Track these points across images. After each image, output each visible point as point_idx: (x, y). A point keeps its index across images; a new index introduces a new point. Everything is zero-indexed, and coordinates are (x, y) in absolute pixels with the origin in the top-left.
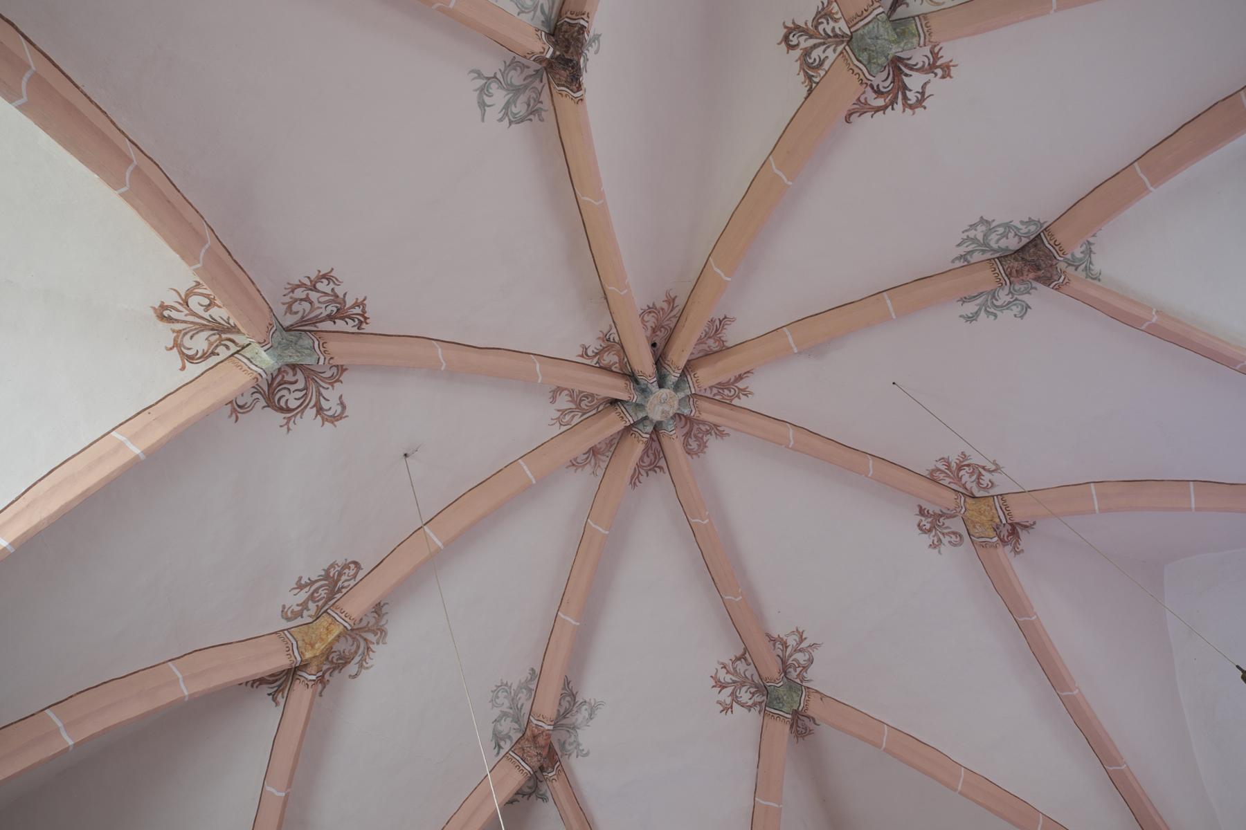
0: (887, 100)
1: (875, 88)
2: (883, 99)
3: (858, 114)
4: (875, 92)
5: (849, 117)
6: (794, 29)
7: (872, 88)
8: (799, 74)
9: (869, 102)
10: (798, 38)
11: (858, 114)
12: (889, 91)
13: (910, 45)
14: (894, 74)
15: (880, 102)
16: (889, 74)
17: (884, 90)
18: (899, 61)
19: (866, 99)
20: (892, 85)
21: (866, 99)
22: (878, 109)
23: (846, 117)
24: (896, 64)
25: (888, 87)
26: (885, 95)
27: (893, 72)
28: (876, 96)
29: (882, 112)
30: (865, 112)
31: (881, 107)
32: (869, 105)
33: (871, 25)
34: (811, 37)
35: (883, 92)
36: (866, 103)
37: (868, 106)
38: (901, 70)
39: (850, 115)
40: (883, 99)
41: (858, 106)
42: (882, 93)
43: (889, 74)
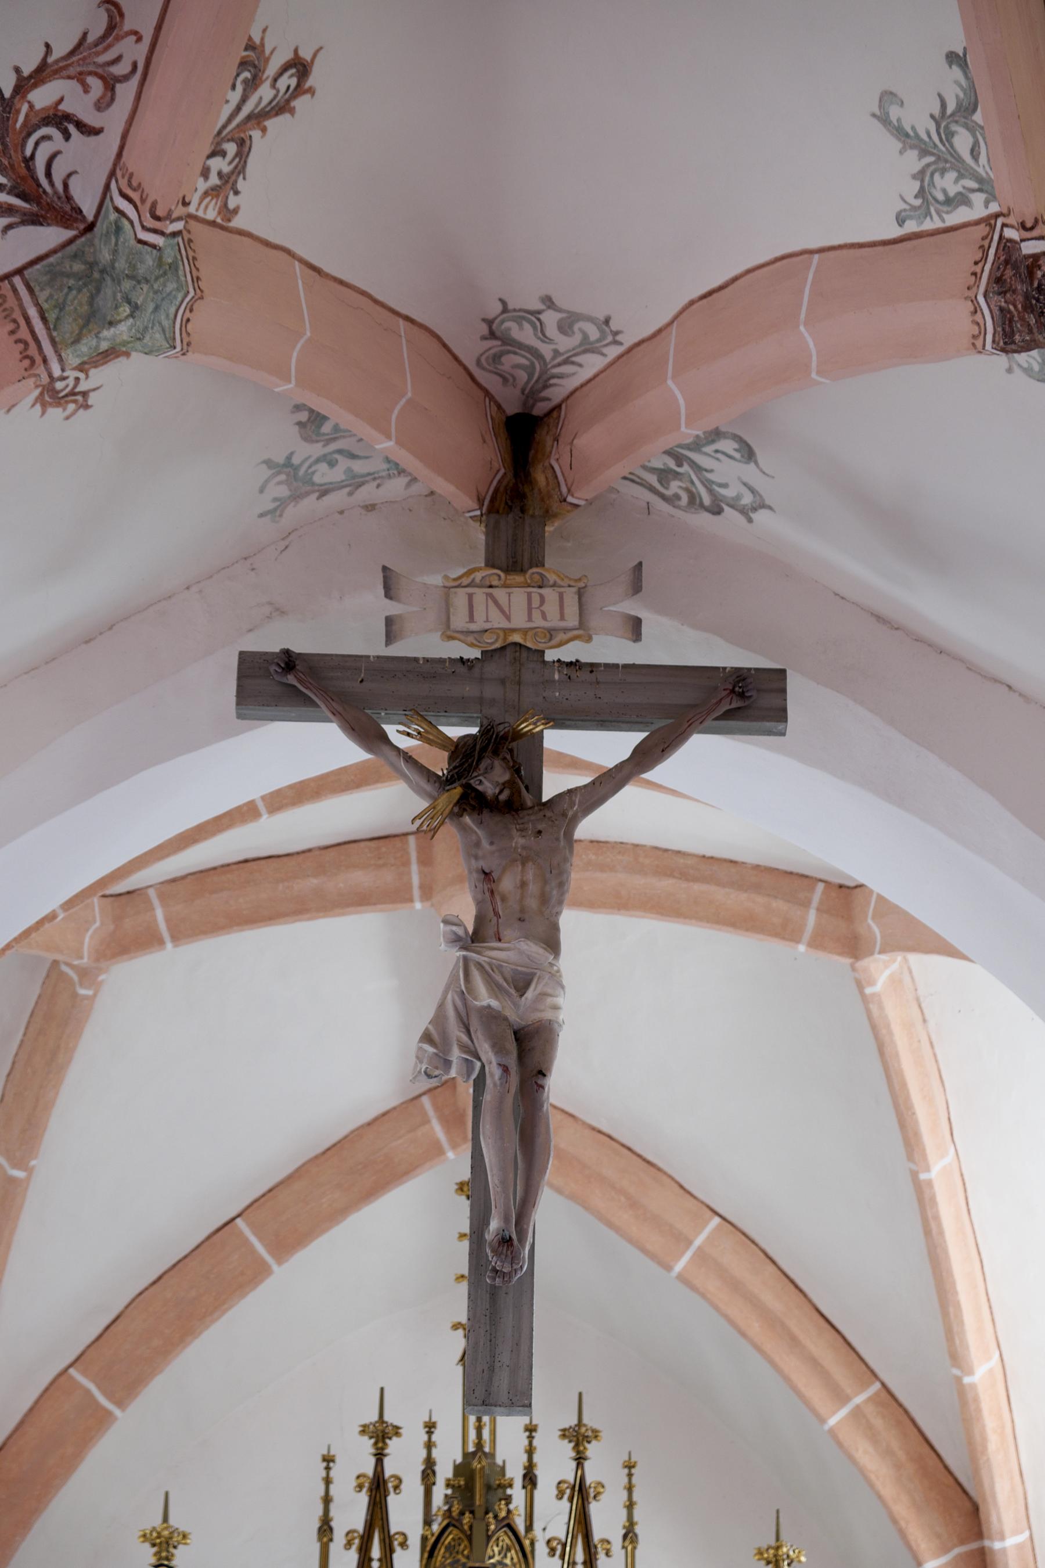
0: (25, 108)
1: (72, 128)
2: (38, 106)
3: (91, 39)
4: (67, 117)
5: (111, 18)
6: (288, 101)
7: (80, 126)
8: (264, 31)
9: (74, 84)
10: (278, 91)
11: (91, 39)
12: (29, 135)
13: (84, 349)
14: (36, 181)
15: (42, 97)
16: (48, 174)
17: (45, 131)
18: (32, 214)
19: (86, 89)
20: (28, 152)
21: (86, 89)
22: (42, 73)
23: (122, 15)
24: (39, 204)
25: (37, 144)
26: (35, 120)
27: (39, 185)
28: (61, 107)
29: (26, 72)
30: (72, 53)
31: (35, 86)
32: (69, 77)
33: (172, 310)
34: (249, 118)
35: (47, 125)
36: (80, 79)
37: (72, 71)
38: (18, 196)
39: (111, 28)
40: (38, 106)
41: (103, 59)
42: (46, 121)
43: (48, 174)
